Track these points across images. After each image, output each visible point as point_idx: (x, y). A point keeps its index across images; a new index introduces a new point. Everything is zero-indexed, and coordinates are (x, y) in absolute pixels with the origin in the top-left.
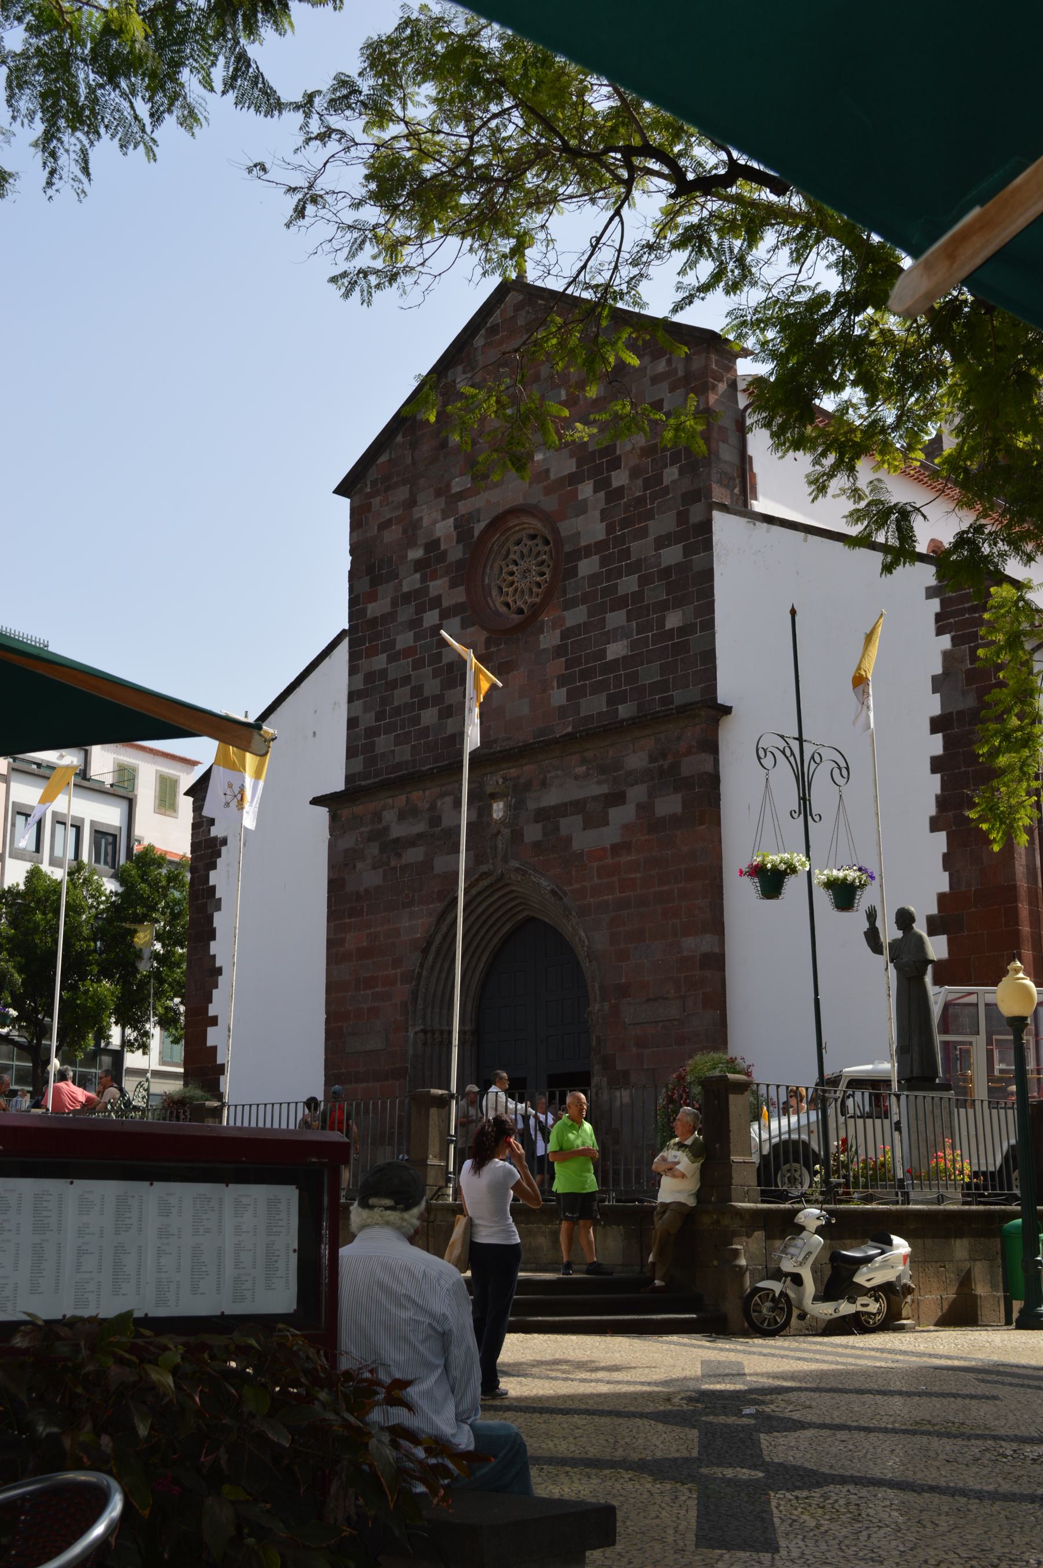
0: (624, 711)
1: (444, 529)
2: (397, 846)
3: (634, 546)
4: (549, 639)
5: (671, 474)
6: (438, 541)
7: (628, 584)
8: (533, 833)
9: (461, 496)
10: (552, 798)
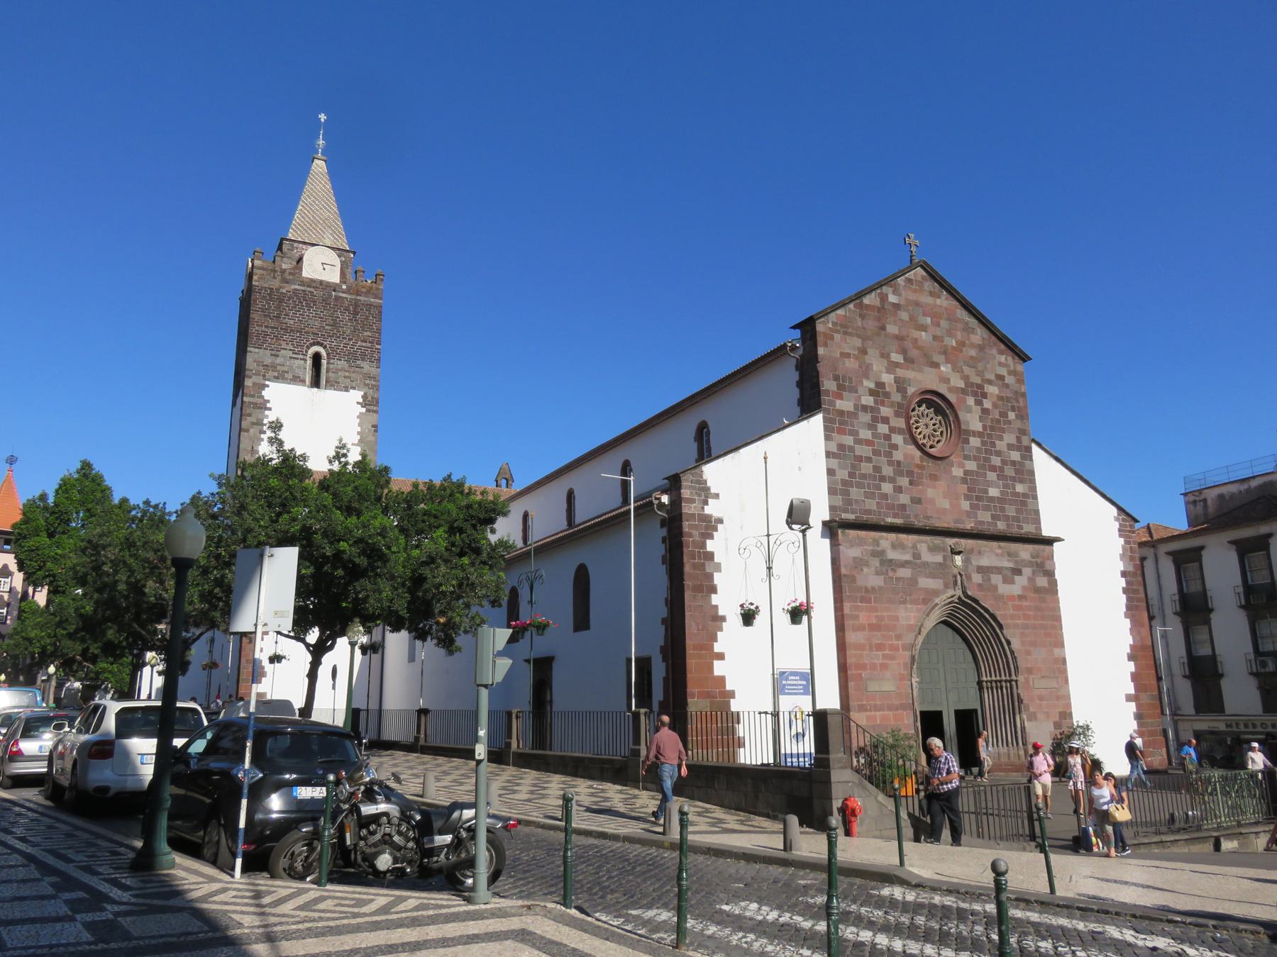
0: (1001, 526)
1: (888, 378)
5: (1012, 416)
6: (883, 384)
7: (996, 461)
8: (977, 578)
9: (897, 365)
10: (985, 562)
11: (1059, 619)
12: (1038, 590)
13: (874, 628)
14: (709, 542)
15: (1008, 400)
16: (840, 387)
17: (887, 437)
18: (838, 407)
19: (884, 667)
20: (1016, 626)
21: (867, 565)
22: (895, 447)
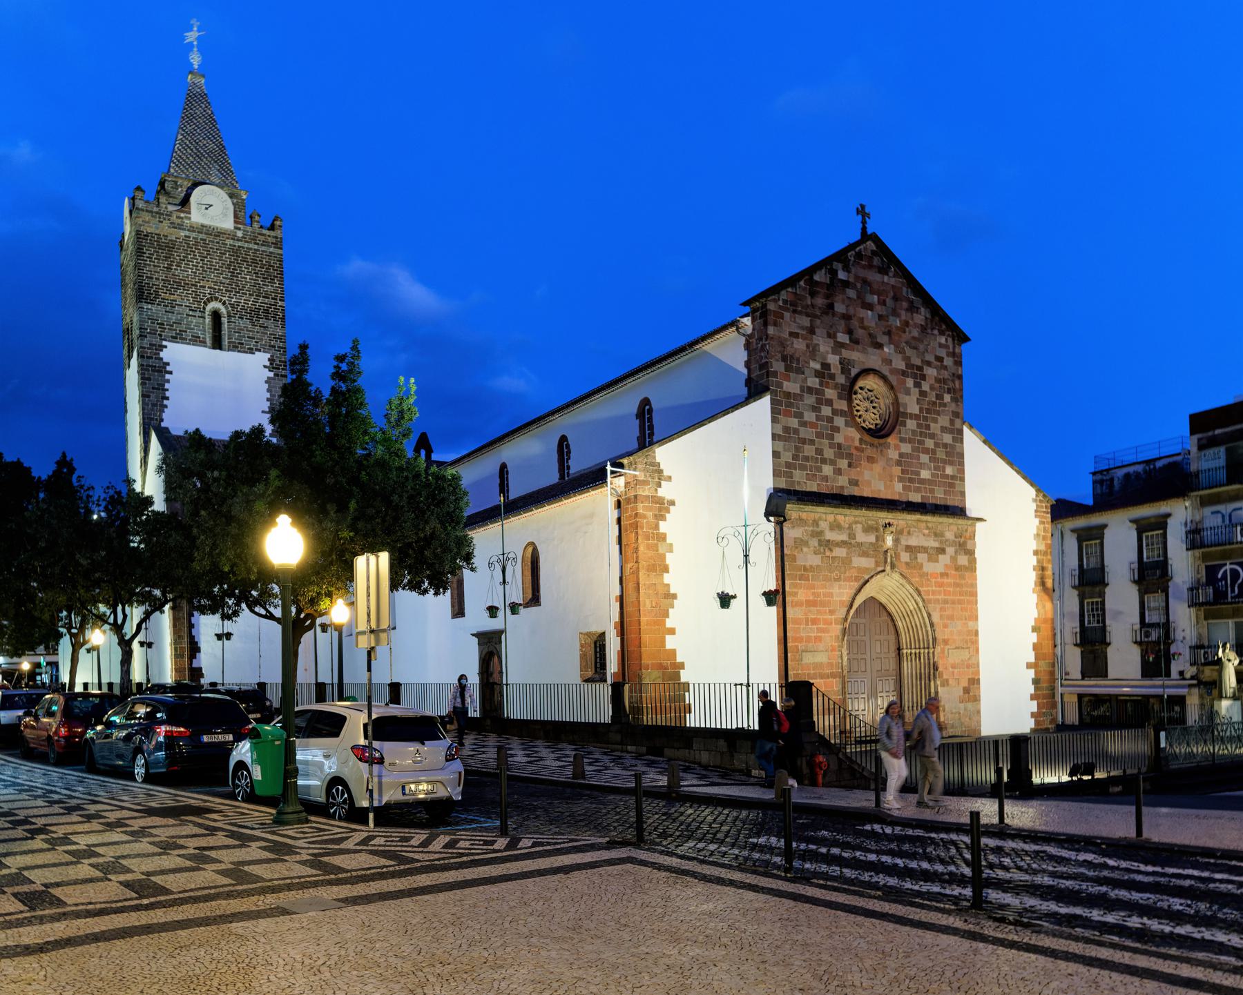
2: (829, 544)
3: (932, 425)
4: (893, 454)
5: (947, 398)
7: (929, 443)
8: (905, 557)
10: (913, 542)
11: (974, 594)
12: (958, 568)
13: (811, 604)
14: (661, 523)
15: (945, 381)
16: (788, 368)
17: (830, 420)
18: (785, 389)
19: (818, 639)
20: (937, 601)
21: (806, 544)
22: (837, 429)
